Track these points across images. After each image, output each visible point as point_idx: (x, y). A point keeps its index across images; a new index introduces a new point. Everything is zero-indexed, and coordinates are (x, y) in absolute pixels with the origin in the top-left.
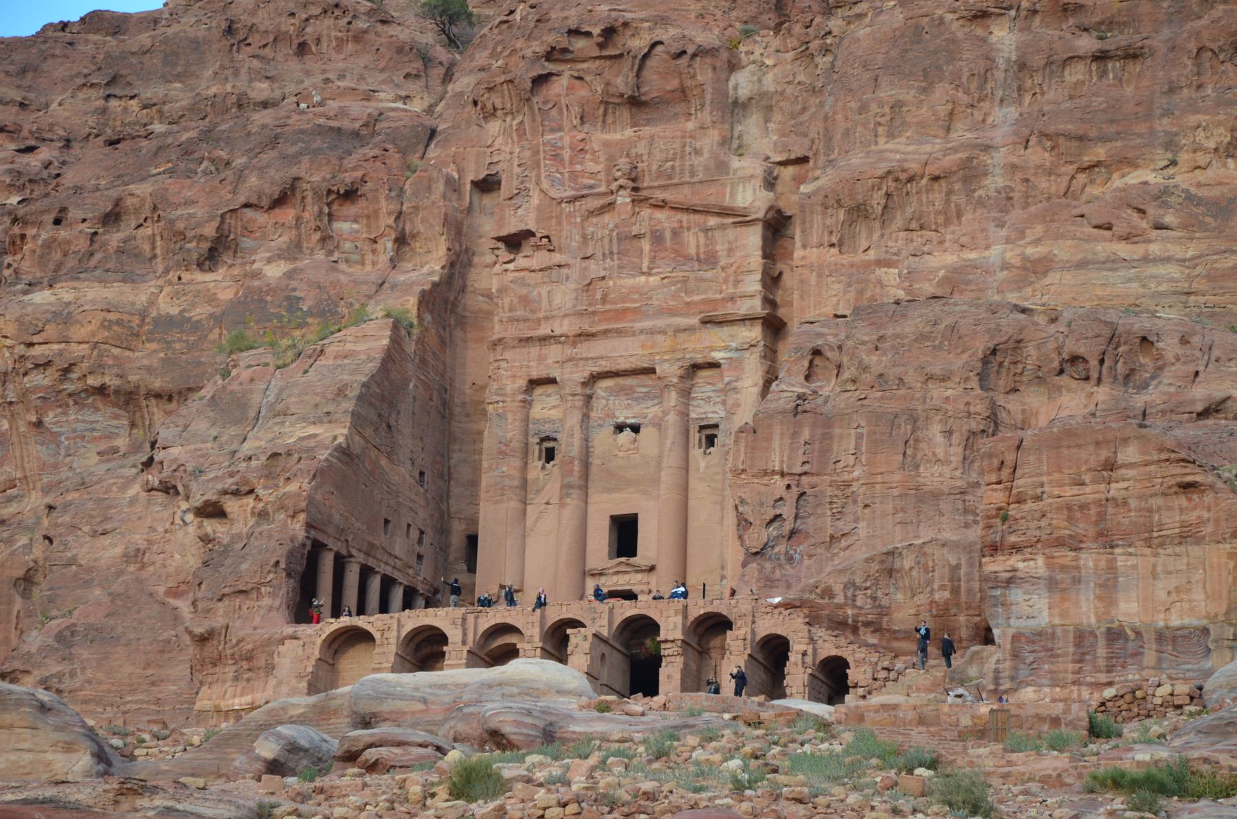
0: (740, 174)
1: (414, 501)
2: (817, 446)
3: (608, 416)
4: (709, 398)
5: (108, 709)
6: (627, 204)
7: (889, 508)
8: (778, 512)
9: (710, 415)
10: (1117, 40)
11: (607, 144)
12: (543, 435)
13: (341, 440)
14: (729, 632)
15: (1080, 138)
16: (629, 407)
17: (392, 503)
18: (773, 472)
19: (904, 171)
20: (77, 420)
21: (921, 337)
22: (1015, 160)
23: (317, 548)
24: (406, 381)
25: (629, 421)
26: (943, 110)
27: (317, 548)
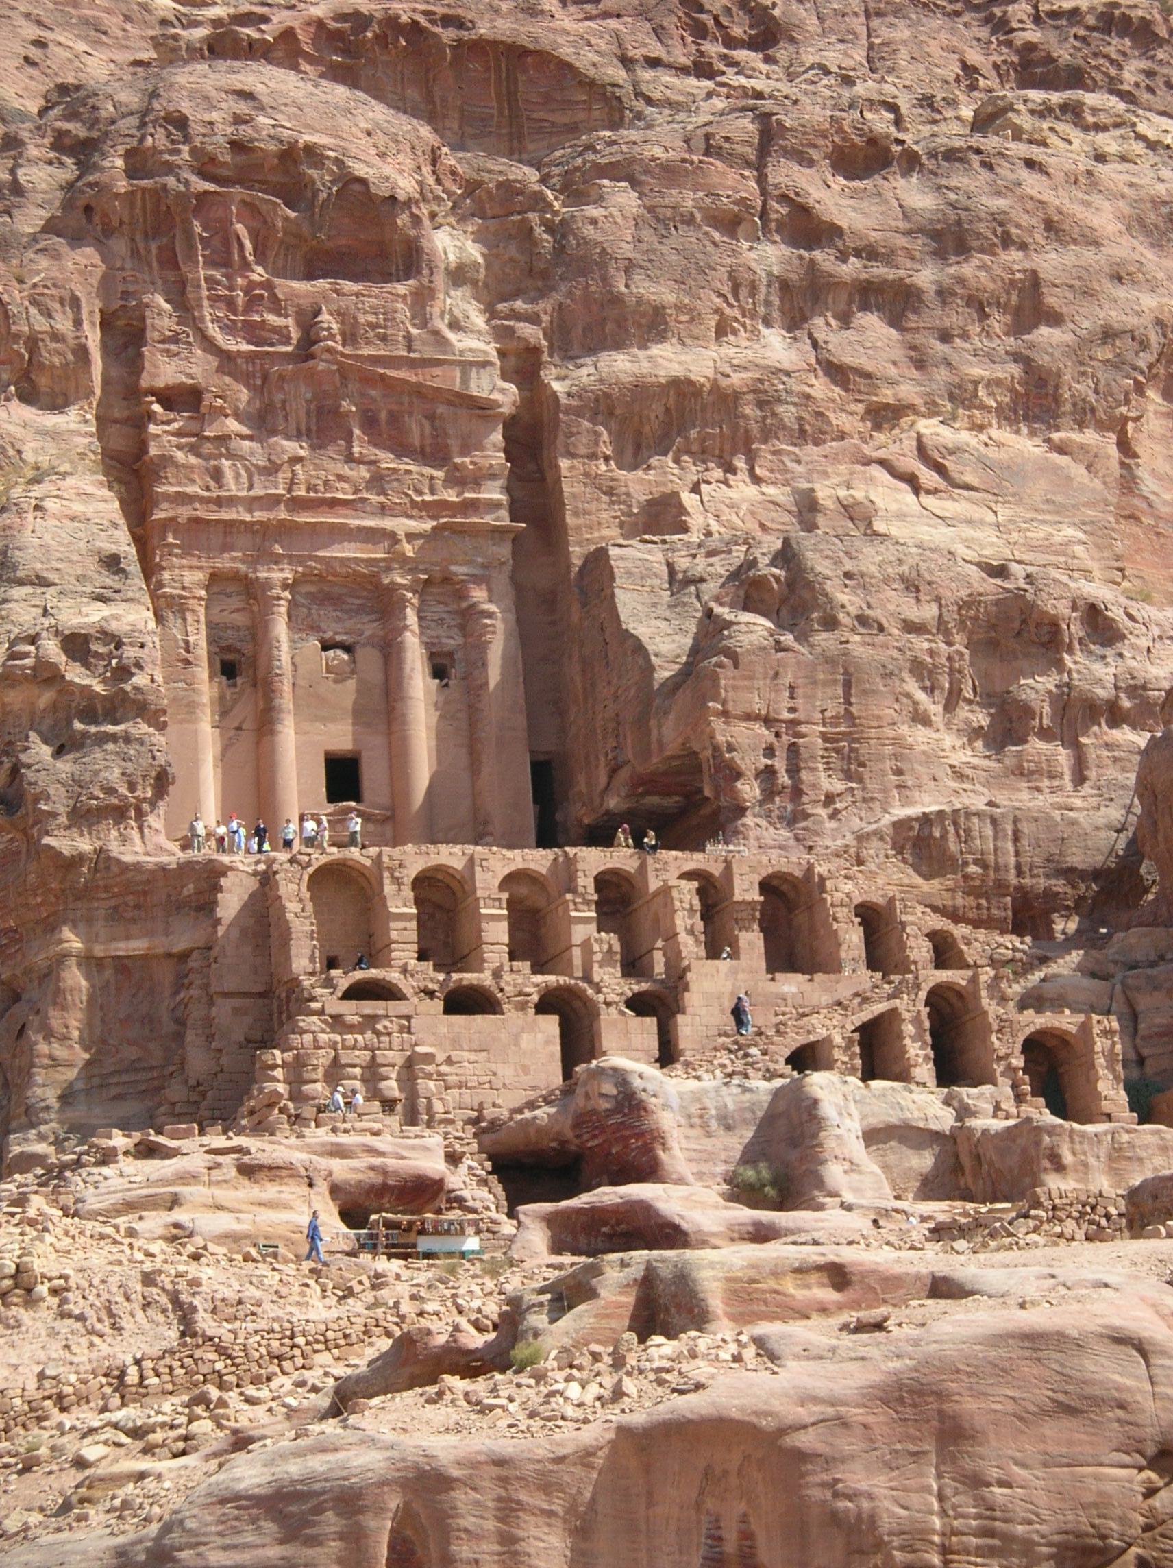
0: (469, 357)
2: (799, 692)
6: (334, 372)
7: (888, 765)
8: (769, 762)
9: (445, 640)
10: (879, 271)
11: (294, 294)
12: (224, 643)
15: (868, 376)
19: (691, 383)
21: (887, 581)
22: (807, 389)
25: (338, 638)
26: (712, 321)
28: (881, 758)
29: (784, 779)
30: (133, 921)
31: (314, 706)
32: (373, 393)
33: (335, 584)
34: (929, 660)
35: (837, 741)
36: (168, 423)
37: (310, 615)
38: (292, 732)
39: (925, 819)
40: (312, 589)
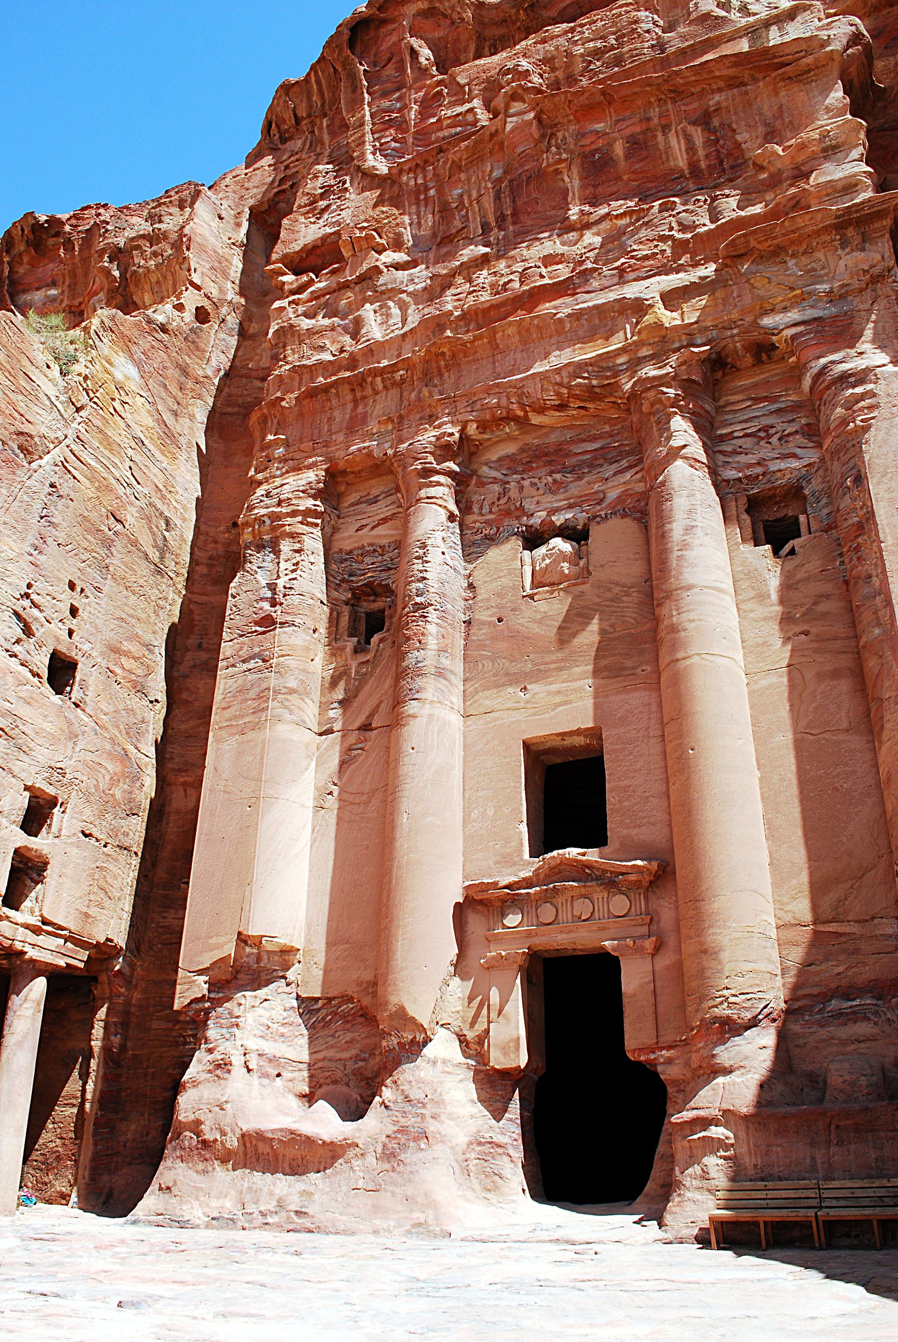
3: (508, 513)
4: (765, 429)
6: (530, 123)
9: (774, 466)
12: (359, 581)
16: (555, 488)
25: (559, 519)
31: (496, 656)
32: (599, 126)
33: (552, 429)
36: (301, 289)
37: (505, 492)
38: (455, 720)
40: (511, 449)
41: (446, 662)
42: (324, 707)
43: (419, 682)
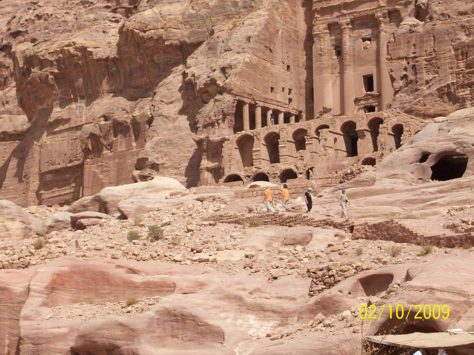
1: (285, 78)
2: (417, 46)
5: (175, 170)
8: (405, 73)
13: (247, 60)
14: (381, 126)
17: (274, 80)
18: (403, 58)
20: (165, 58)
23: (240, 104)
24: (277, 32)
27: (240, 104)
28: (445, 64)
29: (411, 77)
30: (216, 157)
34: (467, 24)
35: (432, 60)
38: (352, 72)
39: (448, 86)
41: (350, 63)
42: (332, 69)
43: (347, 67)
